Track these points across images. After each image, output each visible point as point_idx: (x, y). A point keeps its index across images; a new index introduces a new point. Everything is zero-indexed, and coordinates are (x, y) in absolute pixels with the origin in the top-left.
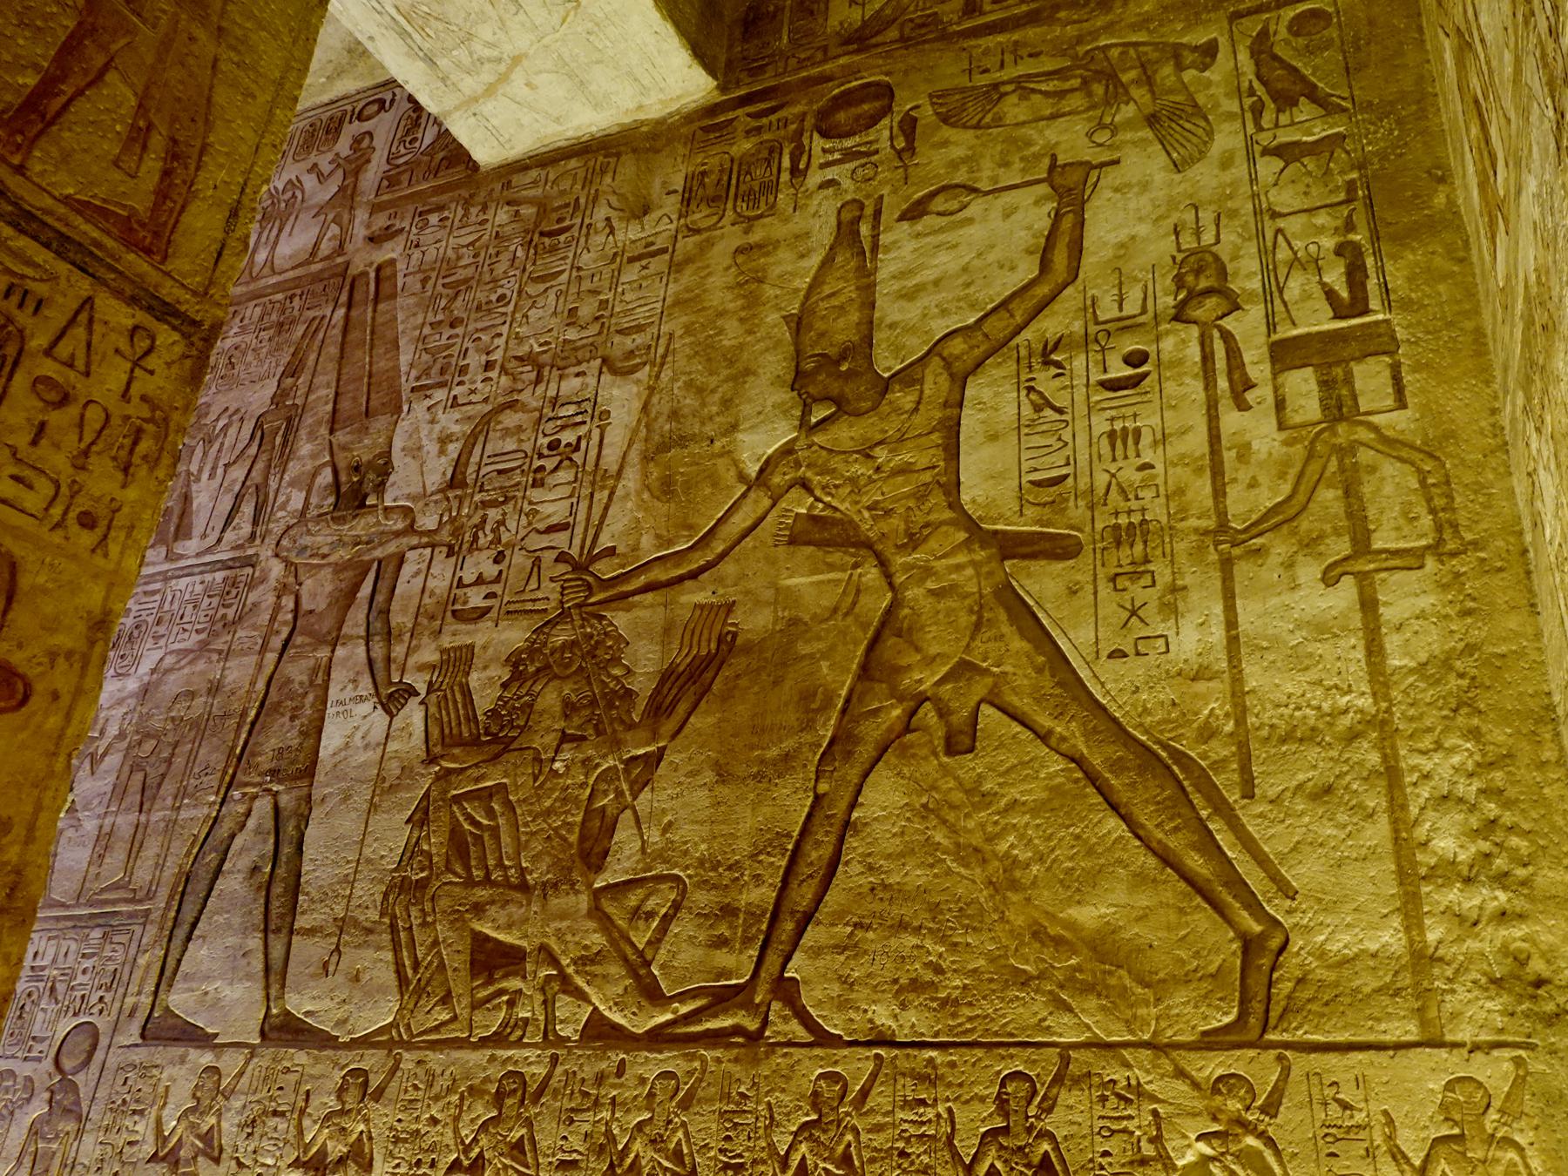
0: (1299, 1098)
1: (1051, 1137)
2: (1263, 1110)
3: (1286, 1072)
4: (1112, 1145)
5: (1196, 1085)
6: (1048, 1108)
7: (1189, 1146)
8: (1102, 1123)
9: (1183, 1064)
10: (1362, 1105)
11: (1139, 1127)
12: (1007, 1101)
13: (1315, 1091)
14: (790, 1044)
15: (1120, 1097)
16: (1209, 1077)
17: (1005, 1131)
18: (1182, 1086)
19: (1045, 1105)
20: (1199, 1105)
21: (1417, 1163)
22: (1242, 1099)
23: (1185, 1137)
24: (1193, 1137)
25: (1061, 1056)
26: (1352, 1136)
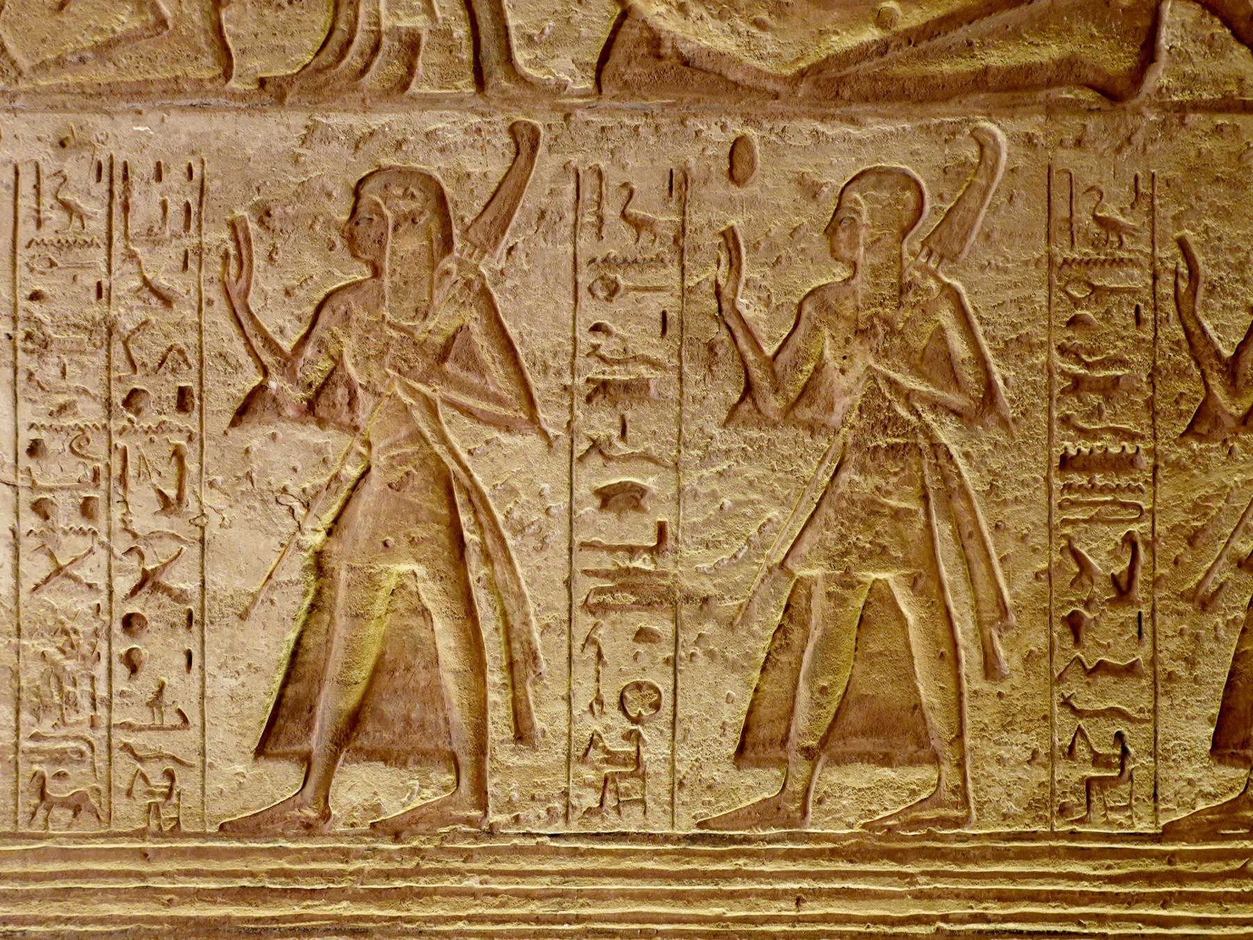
14: (1226, 105)
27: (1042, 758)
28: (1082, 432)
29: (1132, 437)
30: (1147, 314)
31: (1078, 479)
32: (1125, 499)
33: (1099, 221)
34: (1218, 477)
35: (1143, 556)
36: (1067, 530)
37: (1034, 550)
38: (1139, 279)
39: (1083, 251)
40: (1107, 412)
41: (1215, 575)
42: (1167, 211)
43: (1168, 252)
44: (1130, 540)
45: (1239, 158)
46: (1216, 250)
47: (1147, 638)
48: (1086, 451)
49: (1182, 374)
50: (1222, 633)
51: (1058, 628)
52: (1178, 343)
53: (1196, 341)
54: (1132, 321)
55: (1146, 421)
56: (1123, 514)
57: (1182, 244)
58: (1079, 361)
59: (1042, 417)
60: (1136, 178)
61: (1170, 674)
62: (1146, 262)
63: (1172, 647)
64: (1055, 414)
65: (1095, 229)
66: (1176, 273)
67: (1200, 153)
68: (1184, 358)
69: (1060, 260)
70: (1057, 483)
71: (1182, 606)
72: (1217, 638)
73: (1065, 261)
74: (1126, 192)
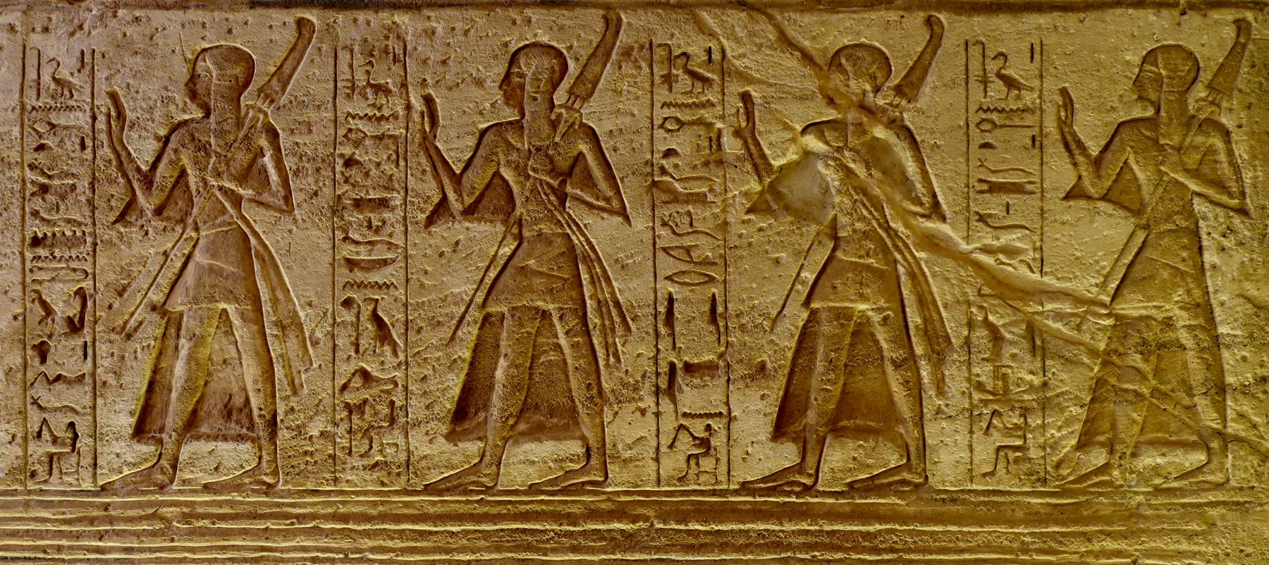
0: (949, 75)
1: (592, 136)
2: (899, 90)
3: (935, 40)
4: (683, 142)
5: (807, 57)
6: (585, 89)
7: (793, 140)
8: (667, 112)
9: (791, 32)
10: (1037, 83)
11: (722, 118)
12: (522, 87)
13: (975, 66)
15: (694, 75)
16: (826, 48)
17: (518, 126)
18: (791, 62)
19: (581, 90)
20: (811, 85)
21: (1094, 152)
22: (873, 78)
23: (787, 127)
24: (799, 128)
25: (606, 20)
26: (1017, 122)
27: (19, 440)
28: (47, 222)
29: (80, 224)
30: (89, 143)
31: (42, 252)
32: (73, 265)
33: (57, 81)
34: (137, 249)
35: (90, 304)
36: (37, 287)
37: (13, 301)
38: (83, 119)
39: (45, 100)
40: (62, 207)
41: (136, 316)
42: (101, 75)
43: (103, 102)
44: (80, 293)
45: (151, 38)
46: (135, 100)
47: (89, 359)
48: (49, 234)
49: (111, 181)
50: (139, 355)
51: (29, 352)
52: (110, 161)
53: (122, 159)
54: (78, 147)
55: (88, 213)
56: (73, 275)
57: (113, 96)
58: (43, 173)
59: (18, 212)
60: (82, 53)
61: (105, 383)
62: (87, 108)
63: (106, 364)
64: (27, 210)
65: (53, 86)
66: (109, 116)
67: (125, 35)
68: (113, 171)
69: (29, 108)
70: (29, 255)
71: (113, 336)
72: (136, 358)
73: (34, 108)
74: (74, 62)
